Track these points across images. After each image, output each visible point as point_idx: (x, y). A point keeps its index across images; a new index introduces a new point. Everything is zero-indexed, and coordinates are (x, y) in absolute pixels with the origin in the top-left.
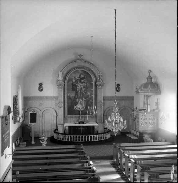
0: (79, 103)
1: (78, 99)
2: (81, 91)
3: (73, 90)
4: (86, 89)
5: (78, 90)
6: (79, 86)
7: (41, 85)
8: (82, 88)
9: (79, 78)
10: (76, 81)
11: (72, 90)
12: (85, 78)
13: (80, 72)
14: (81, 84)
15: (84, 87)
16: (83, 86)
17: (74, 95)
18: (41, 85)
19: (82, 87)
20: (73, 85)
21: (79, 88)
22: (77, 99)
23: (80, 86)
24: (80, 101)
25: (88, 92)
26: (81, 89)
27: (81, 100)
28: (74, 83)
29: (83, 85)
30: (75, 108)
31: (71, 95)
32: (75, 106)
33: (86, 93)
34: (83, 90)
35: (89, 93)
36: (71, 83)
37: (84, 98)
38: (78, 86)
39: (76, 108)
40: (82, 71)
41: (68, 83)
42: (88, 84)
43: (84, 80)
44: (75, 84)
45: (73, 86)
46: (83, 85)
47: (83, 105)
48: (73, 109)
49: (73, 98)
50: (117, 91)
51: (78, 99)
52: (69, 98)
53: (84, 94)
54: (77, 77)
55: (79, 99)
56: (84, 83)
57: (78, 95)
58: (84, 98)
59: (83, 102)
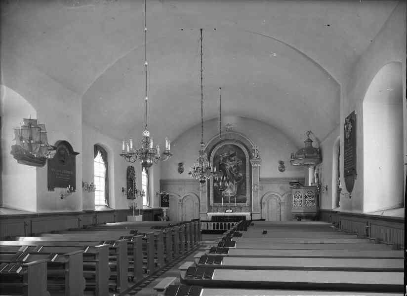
6: (228, 164)
7: (181, 164)
12: (235, 155)
13: (230, 147)
14: (231, 163)
15: (234, 167)
18: (181, 164)
19: (232, 166)
23: (229, 165)
25: (241, 173)
26: (231, 168)
27: (231, 183)
35: (241, 174)
40: (231, 145)
43: (235, 157)
47: (234, 189)
50: (281, 171)
53: (235, 175)
56: (235, 161)
58: (235, 181)
59: (234, 186)
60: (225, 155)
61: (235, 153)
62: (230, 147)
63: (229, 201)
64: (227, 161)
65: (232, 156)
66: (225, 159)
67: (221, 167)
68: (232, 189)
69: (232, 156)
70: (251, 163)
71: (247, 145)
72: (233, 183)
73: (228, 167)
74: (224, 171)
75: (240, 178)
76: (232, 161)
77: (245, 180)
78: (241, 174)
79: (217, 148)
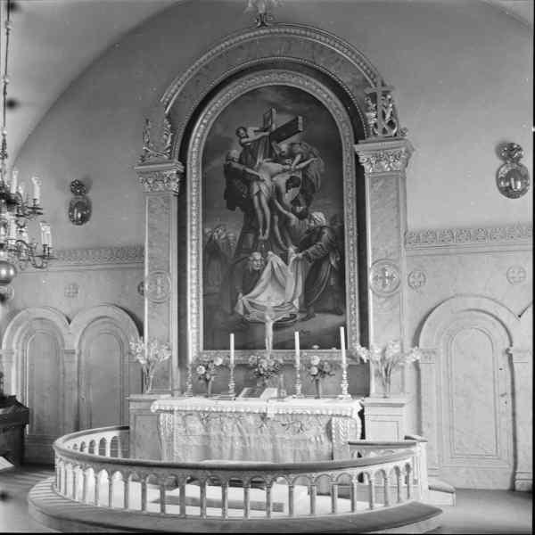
0: (265, 275)
1: (257, 256)
2: (271, 203)
3: (231, 207)
4: (302, 191)
5: (256, 198)
6: (264, 175)
8: (283, 189)
9: (265, 131)
10: (249, 152)
11: (225, 202)
13: (272, 97)
14: (276, 167)
15: (291, 183)
16: (287, 176)
17: (238, 234)
19: (282, 181)
20: (229, 172)
21: (264, 188)
22: (250, 252)
23: (269, 177)
24: (268, 268)
26: (277, 193)
27: (275, 259)
28: (236, 165)
29: (284, 171)
30: (246, 312)
31: (220, 235)
32: (241, 295)
33: (301, 216)
34: (288, 197)
35: (319, 217)
36: (219, 162)
37: (292, 249)
38: (258, 179)
39: (250, 309)
40: (278, 88)
41: (205, 162)
42: (317, 166)
43: (294, 139)
44: (241, 167)
45: (229, 183)
46: (284, 171)
48: (233, 313)
49: (234, 245)
51: (257, 256)
52: (211, 251)
54: (250, 131)
55: (265, 255)
56: (292, 155)
57: (257, 234)
58: (292, 249)
59: (290, 272)
60: (252, 134)
61: (297, 119)
62: (272, 97)
63: (269, 341)
64: (259, 160)
65: (288, 131)
66: (249, 152)
67: (231, 189)
68: (282, 288)
69: (288, 131)
70: (363, 159)
71: (332, 71)
72: (285, 258)
73: (263, 189)
74: (250, 212)
75: (315, 233)
76: (278, 159)
77: (337, 245)
78: (319, 217)
79: (218, 103)
